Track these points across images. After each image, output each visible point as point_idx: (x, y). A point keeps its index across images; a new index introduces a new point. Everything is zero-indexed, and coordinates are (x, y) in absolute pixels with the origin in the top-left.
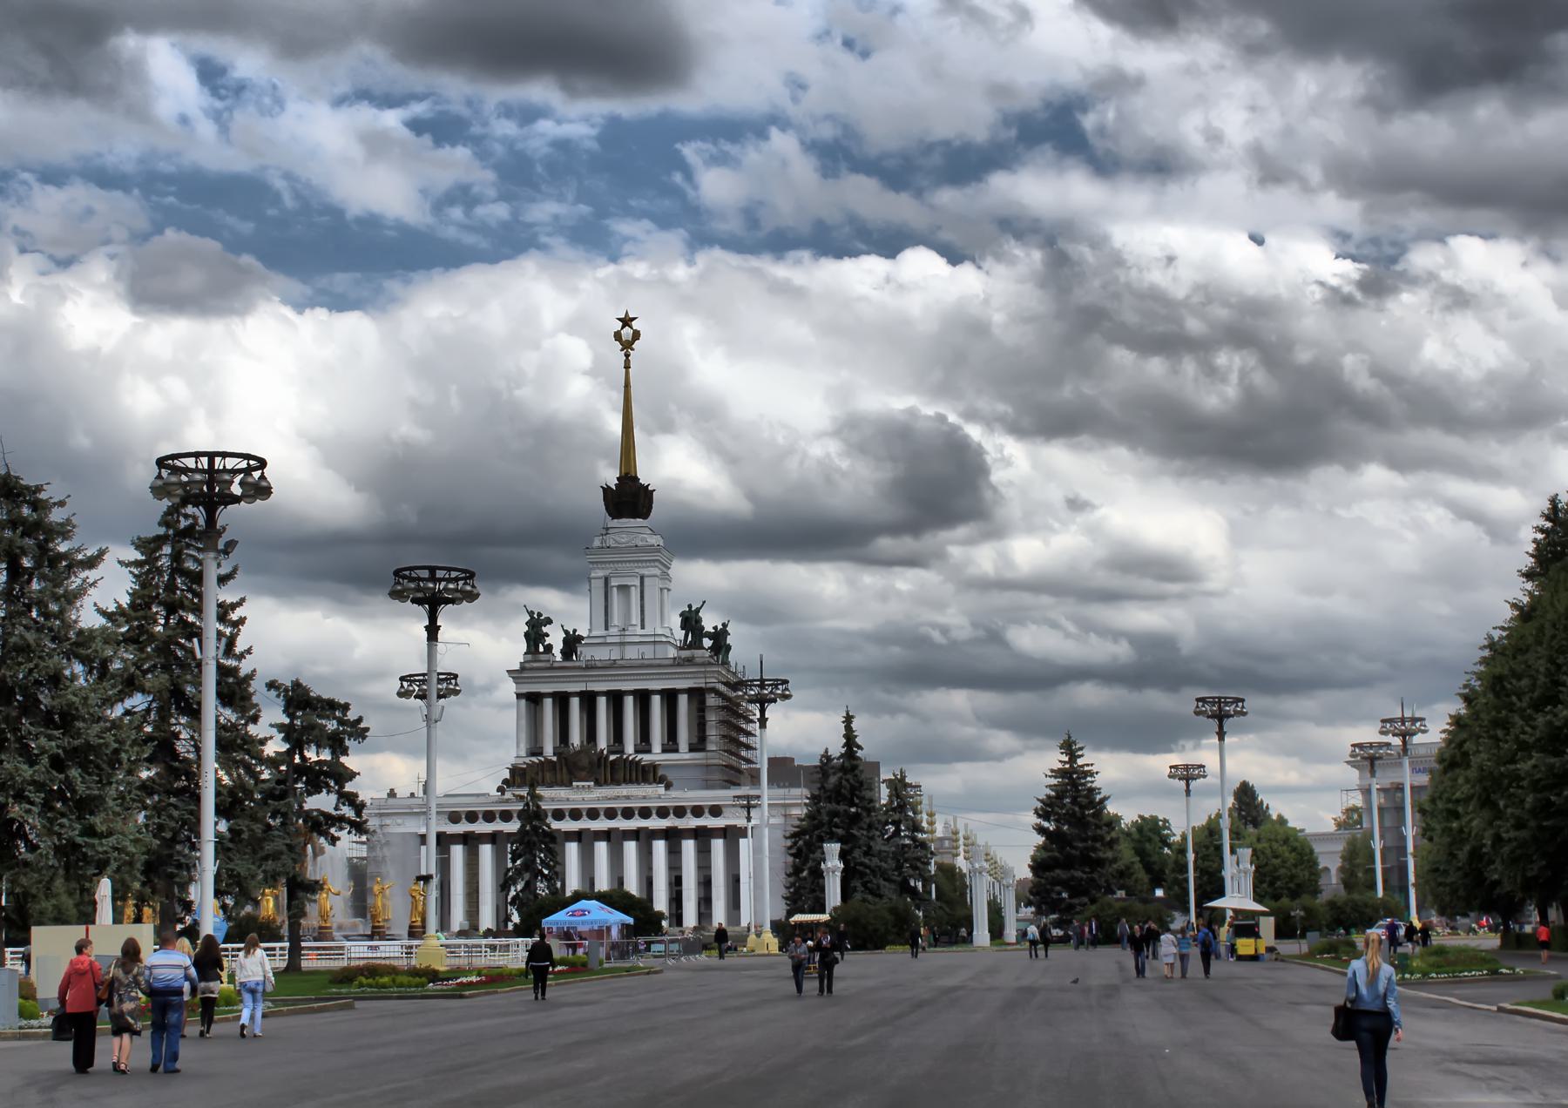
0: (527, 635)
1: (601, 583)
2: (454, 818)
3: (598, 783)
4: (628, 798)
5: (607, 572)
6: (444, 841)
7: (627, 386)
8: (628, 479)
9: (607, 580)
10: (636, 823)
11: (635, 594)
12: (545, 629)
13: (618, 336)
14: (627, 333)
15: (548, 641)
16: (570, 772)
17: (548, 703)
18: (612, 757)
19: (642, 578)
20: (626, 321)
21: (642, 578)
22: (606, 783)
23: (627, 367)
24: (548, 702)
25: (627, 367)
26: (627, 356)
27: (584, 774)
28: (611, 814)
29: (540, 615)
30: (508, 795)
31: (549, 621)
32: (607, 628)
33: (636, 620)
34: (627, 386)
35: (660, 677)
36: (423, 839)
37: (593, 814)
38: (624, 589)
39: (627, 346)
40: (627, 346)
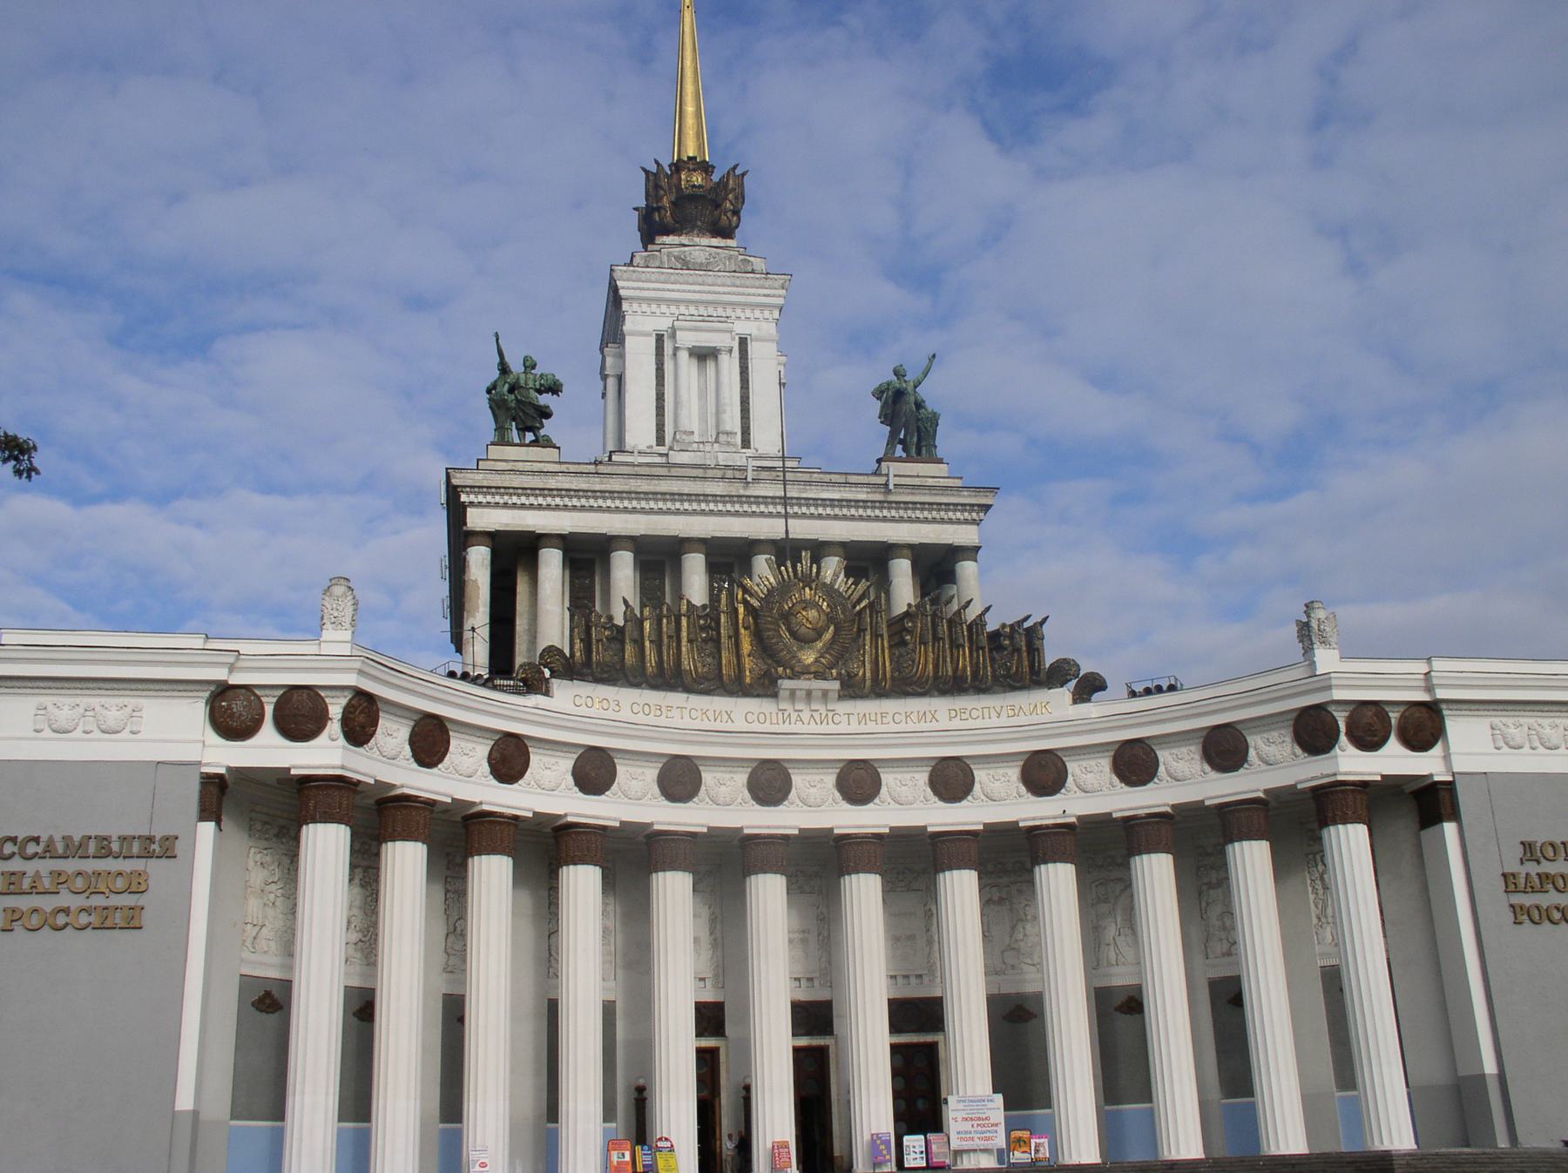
0: (498, 406)
1: (653, 340)
3: (852, 690)
5: (664, 324)
9: (660, 339)
11: (729, 366)
12: (545, 399)
15: (549, 428)
16: (764, 647)
17: (551, 563)
19: (743, 342)
21: (743, 342)
22: (879, 690)
24: (551, 563)
27: (809, 657)
29: (529, 365)
31: (555, 389)
32: (660, 440)
33: (733, 422)
38: (704, 355)
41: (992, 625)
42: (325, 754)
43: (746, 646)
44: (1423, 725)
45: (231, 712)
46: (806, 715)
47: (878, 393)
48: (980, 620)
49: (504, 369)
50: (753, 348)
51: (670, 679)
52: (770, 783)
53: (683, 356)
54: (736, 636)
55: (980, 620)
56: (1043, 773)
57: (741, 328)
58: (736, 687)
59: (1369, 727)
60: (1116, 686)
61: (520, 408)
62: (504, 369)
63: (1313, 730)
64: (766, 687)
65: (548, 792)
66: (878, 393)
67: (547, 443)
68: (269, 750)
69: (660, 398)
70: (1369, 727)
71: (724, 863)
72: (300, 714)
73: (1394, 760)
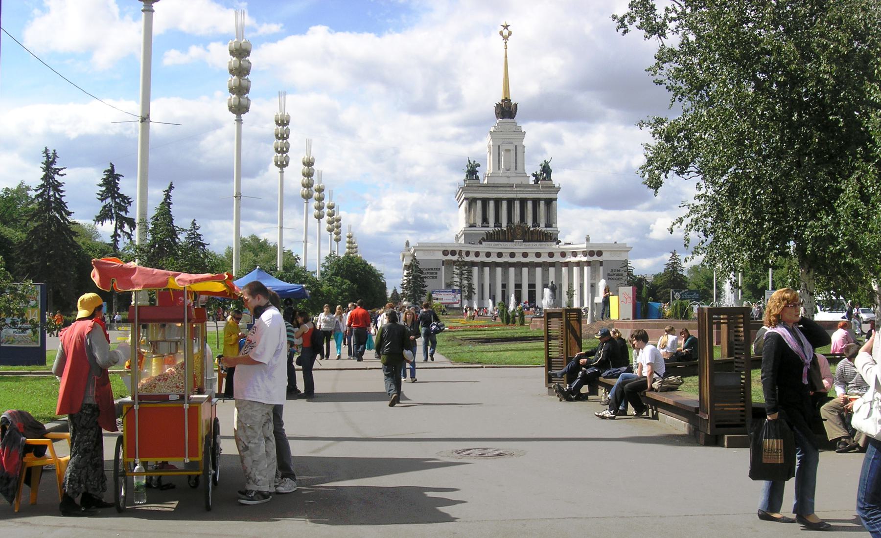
8: (507, 100)
12: (477, 169)
13: (501, 33)
14: (506, 33)
15: (478, 174)
18: (532, 229)
20: (506, 27)
22: (529, 241)
24: (479, 203)
33: (513, 165)
35: (531, 192)
39: (506, 38)
42: (455, 258)
44: (600, 253)
45: (445, 253)
51: (499, 240)
52: (512, 255)
56: (551, 255)
59: (591, 253)
60: (563, 243)
61: (472, 172)
63: (585, 254)
64: (512, 241)
65: (482, 258)
67: (477, 178)
68: (450, 257)
70: (591, 253)
71: (506, 266)
72: (453, 253)
73: (595, 258)
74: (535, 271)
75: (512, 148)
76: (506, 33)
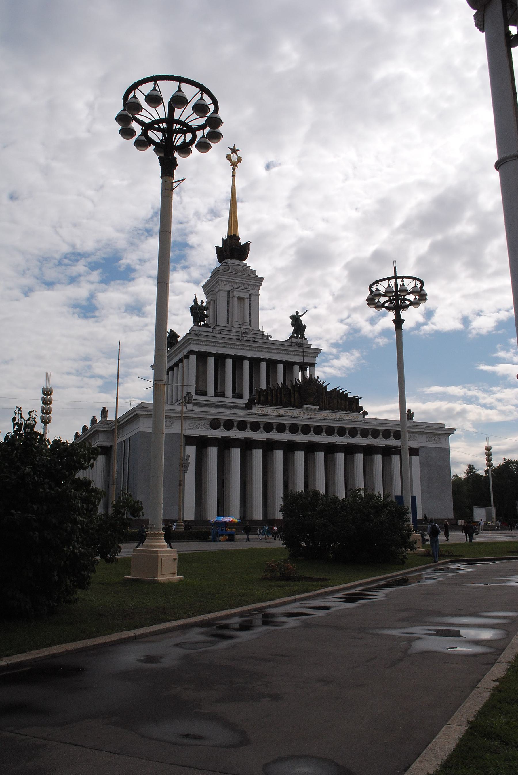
2: (215, 424)
4: (343, 420)
5: (229, 288)
6: (202, 443)
7: (233, 186)
9: (228, 292)
10: (346, 440)
19: (250, 295)
20: (234, 151)
23: (234, 176)
25: (234, 176)
26: (234, 169)
28: (330, 431)
30: (255, 410)
32: (228, 323)
34: (233, 186)
36: (189, 440)
37: (318, 430)
38: (241, 299)
40: (234, 164)
41: (350, 395)
43: (296, 397)
46: (310, 414)
47: (292, 317)
48: (347, 394)
49: (195, 301)
50: (253, 298)
53: (235, 299)
54: (294, 394)
55: (347, 394)
57: (251, 291)
58: (294, 406)
62: (195, 301)
66: (292, 317)
69: (228, 310)
74: (333, 460)
75: (246, 295)
76: (234, 157)
